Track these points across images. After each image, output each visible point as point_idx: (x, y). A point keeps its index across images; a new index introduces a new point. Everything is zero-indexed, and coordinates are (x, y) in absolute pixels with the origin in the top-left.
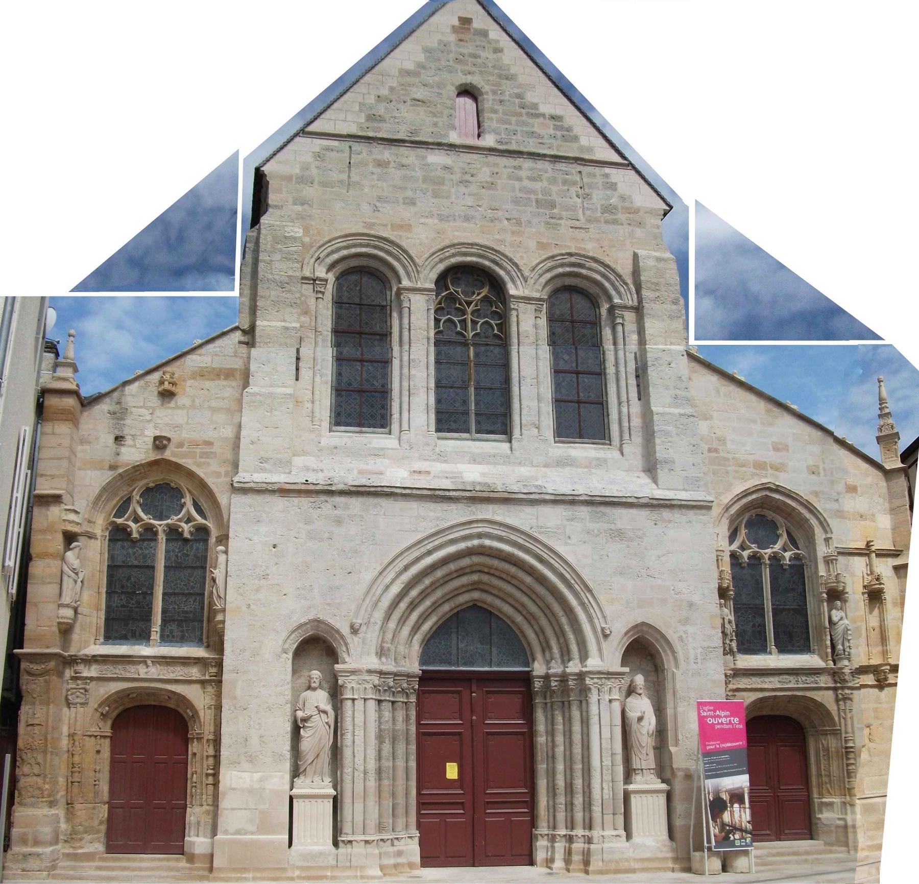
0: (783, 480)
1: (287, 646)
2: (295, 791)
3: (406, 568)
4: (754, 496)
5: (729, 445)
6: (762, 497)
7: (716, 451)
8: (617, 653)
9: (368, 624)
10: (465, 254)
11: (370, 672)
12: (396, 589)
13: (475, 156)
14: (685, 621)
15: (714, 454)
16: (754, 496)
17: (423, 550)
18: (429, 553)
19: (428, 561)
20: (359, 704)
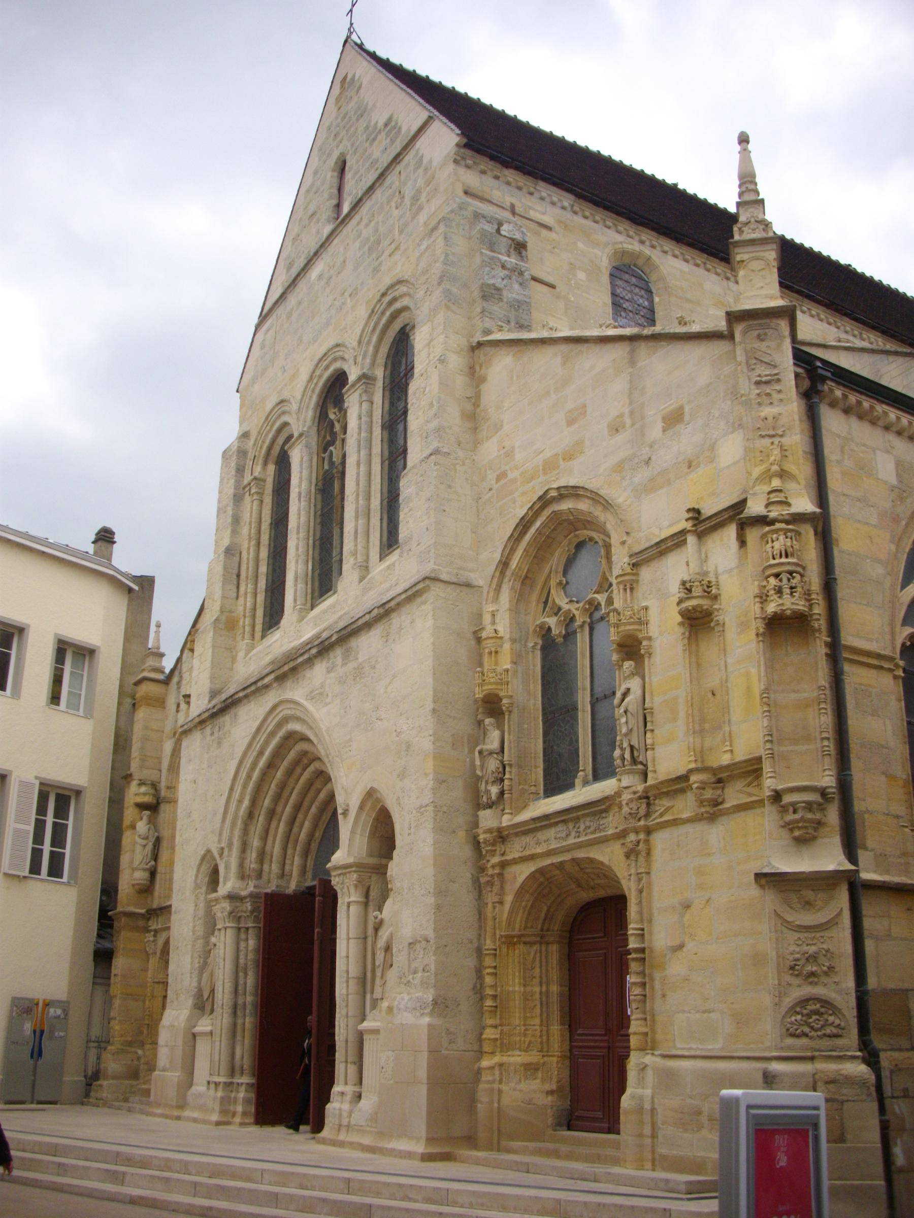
0: (573, 475)
1: (199, 881)
2: (197, 1029)
3: (249, 777)
4: (538, 524)
5: (519, 456)
6: (550, 518)
7: (504, 475)
8: (358, 837)
9: (230, 845)
10: (327, 367)
11: (224, 898)
12: (246, 803)
13: (335, 241)
14: (402, 775)
15: (502, 482)
16: (538, 524)
17: (255, 753)
18: (261, 753)
19: (262, 762)
20: (223, 932)
